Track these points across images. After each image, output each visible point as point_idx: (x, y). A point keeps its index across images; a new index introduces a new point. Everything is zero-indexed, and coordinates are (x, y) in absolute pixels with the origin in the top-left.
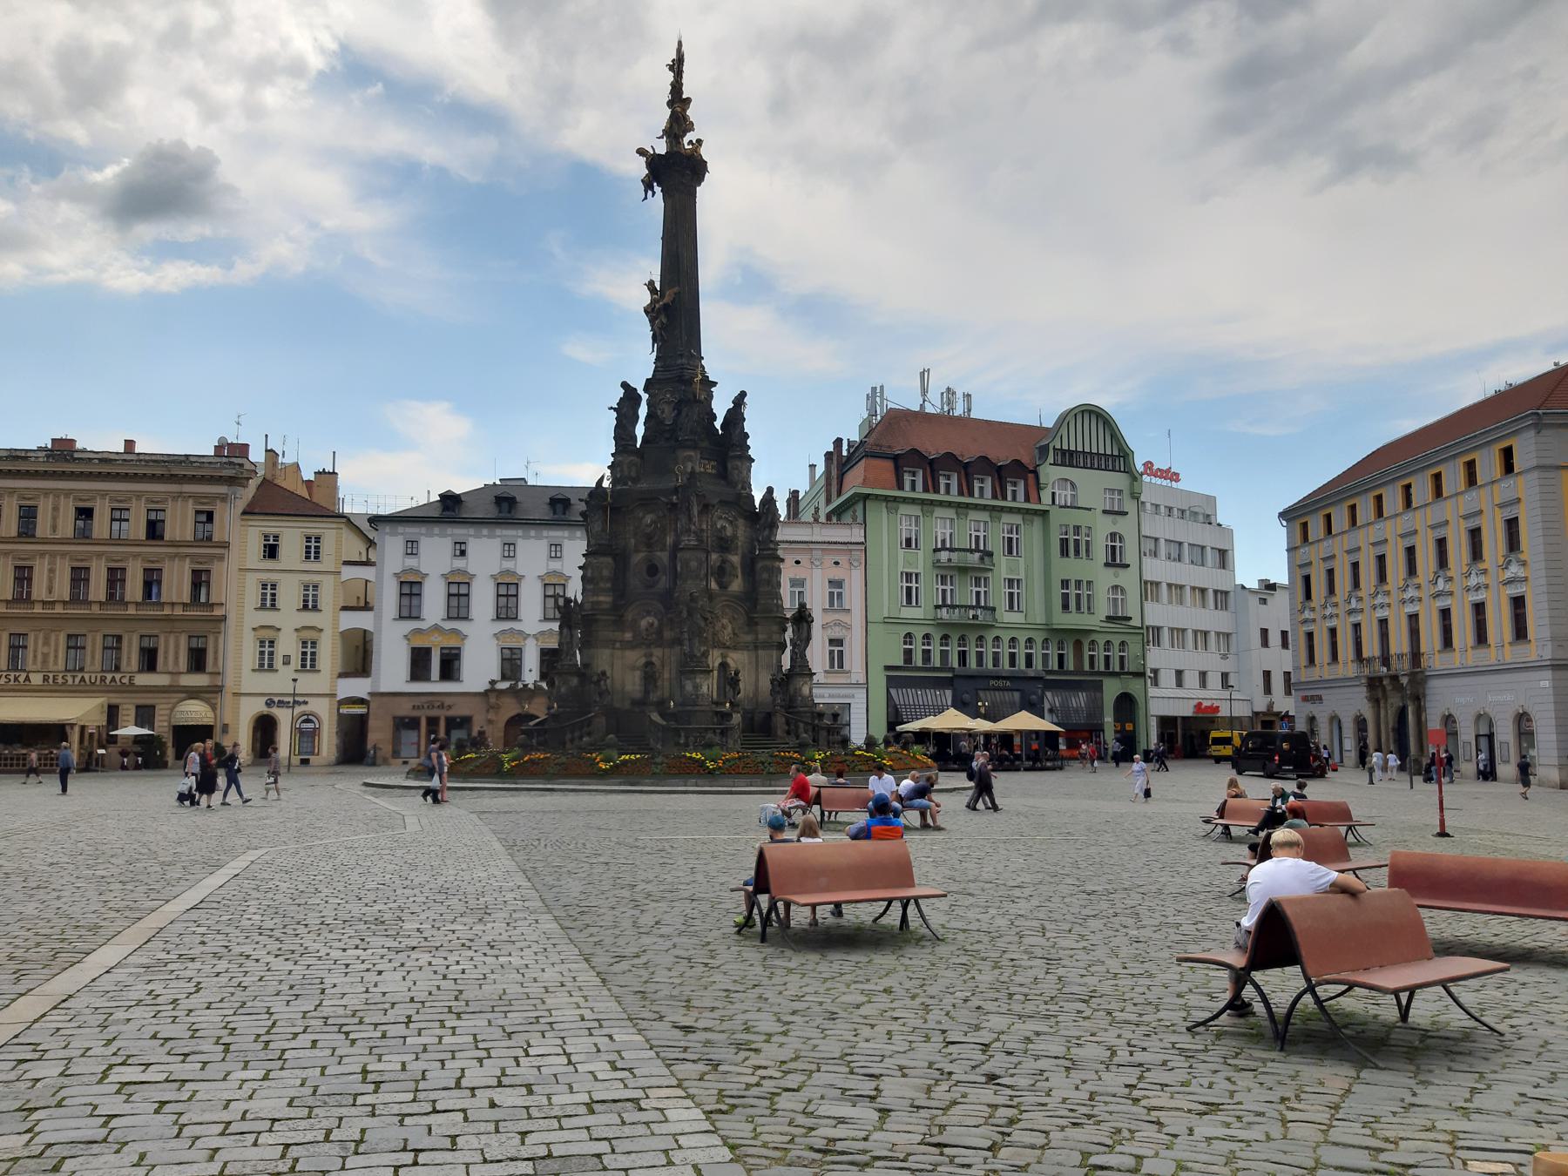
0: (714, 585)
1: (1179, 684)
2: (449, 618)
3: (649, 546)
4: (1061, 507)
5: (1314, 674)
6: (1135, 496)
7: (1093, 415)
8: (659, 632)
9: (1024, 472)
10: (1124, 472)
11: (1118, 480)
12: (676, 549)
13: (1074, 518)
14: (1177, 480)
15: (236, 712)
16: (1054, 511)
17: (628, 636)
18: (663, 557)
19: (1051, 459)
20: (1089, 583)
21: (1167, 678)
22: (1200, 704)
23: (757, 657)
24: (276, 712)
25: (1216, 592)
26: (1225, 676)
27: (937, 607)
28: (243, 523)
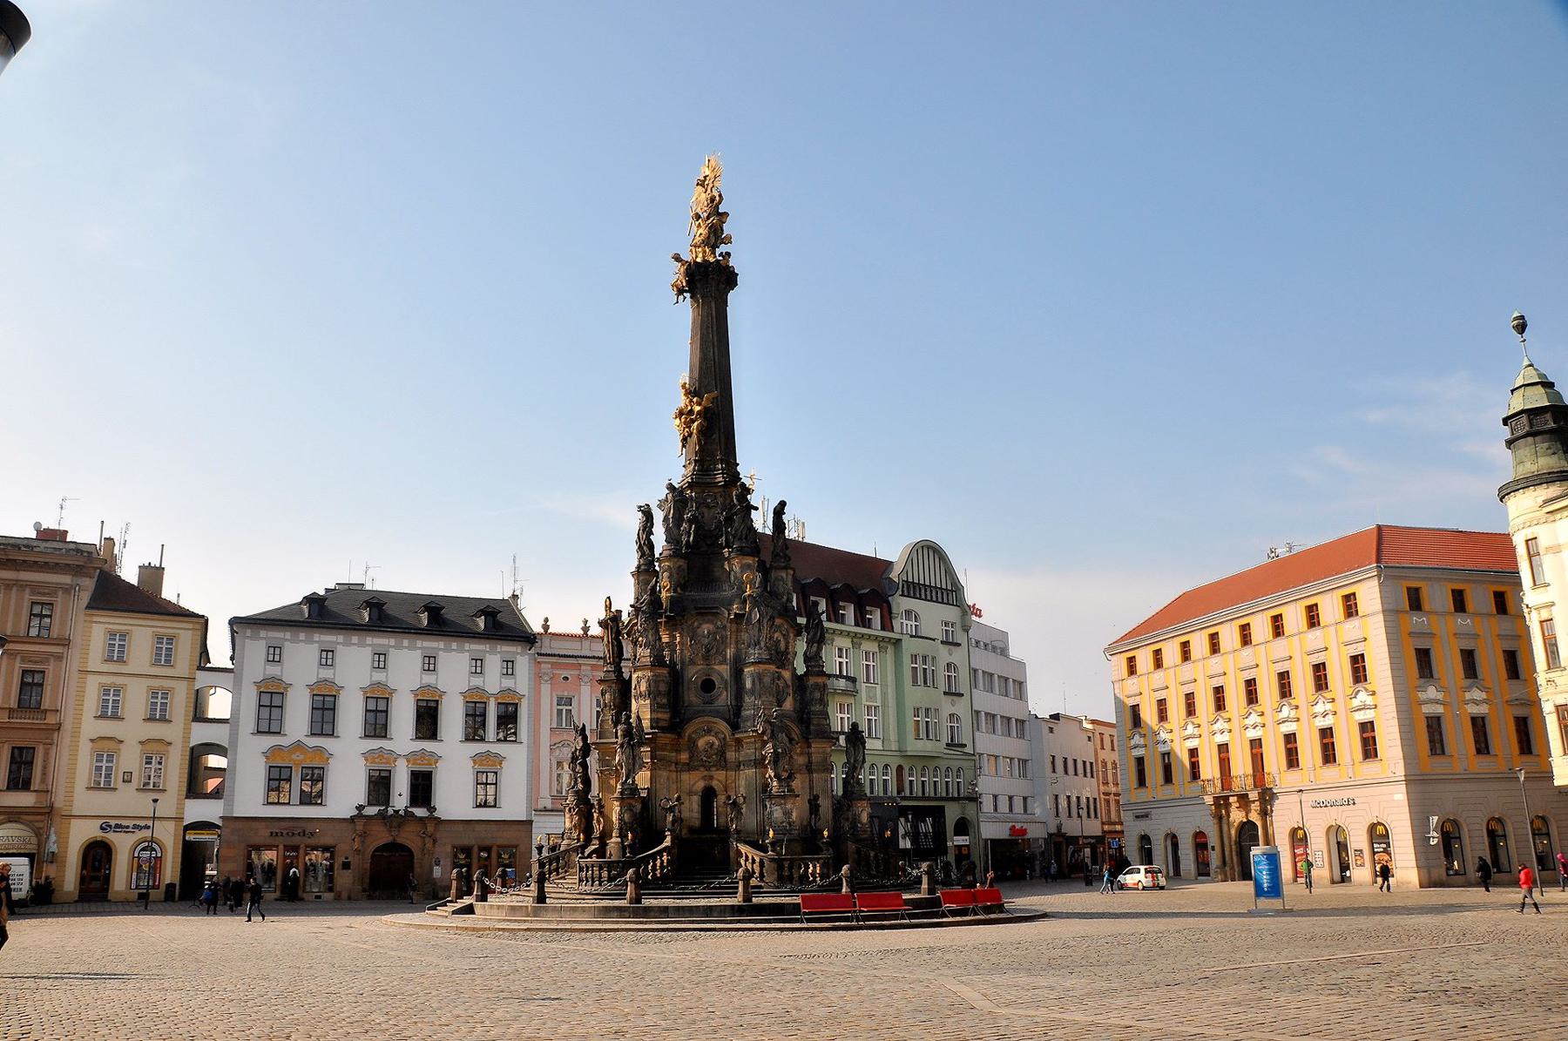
3: (706, 658)
4: (912, 636)
5: (1142, 795)
6: (966, 629)
7: (930, 551)
9: (880, 598)
10: (956, 605)
11: (951, 613)
14: (980, 616)
15: (63, 841)
16: (905, 638)
17: (684, 757)
18: (724, 670)
19: (900, 592)
20: (937, 710)
21: (987, 804)
22: (1014, 826)
23: (811, 781)
24: (112, 837)
25: (1016, 720)
28: (88, 618)
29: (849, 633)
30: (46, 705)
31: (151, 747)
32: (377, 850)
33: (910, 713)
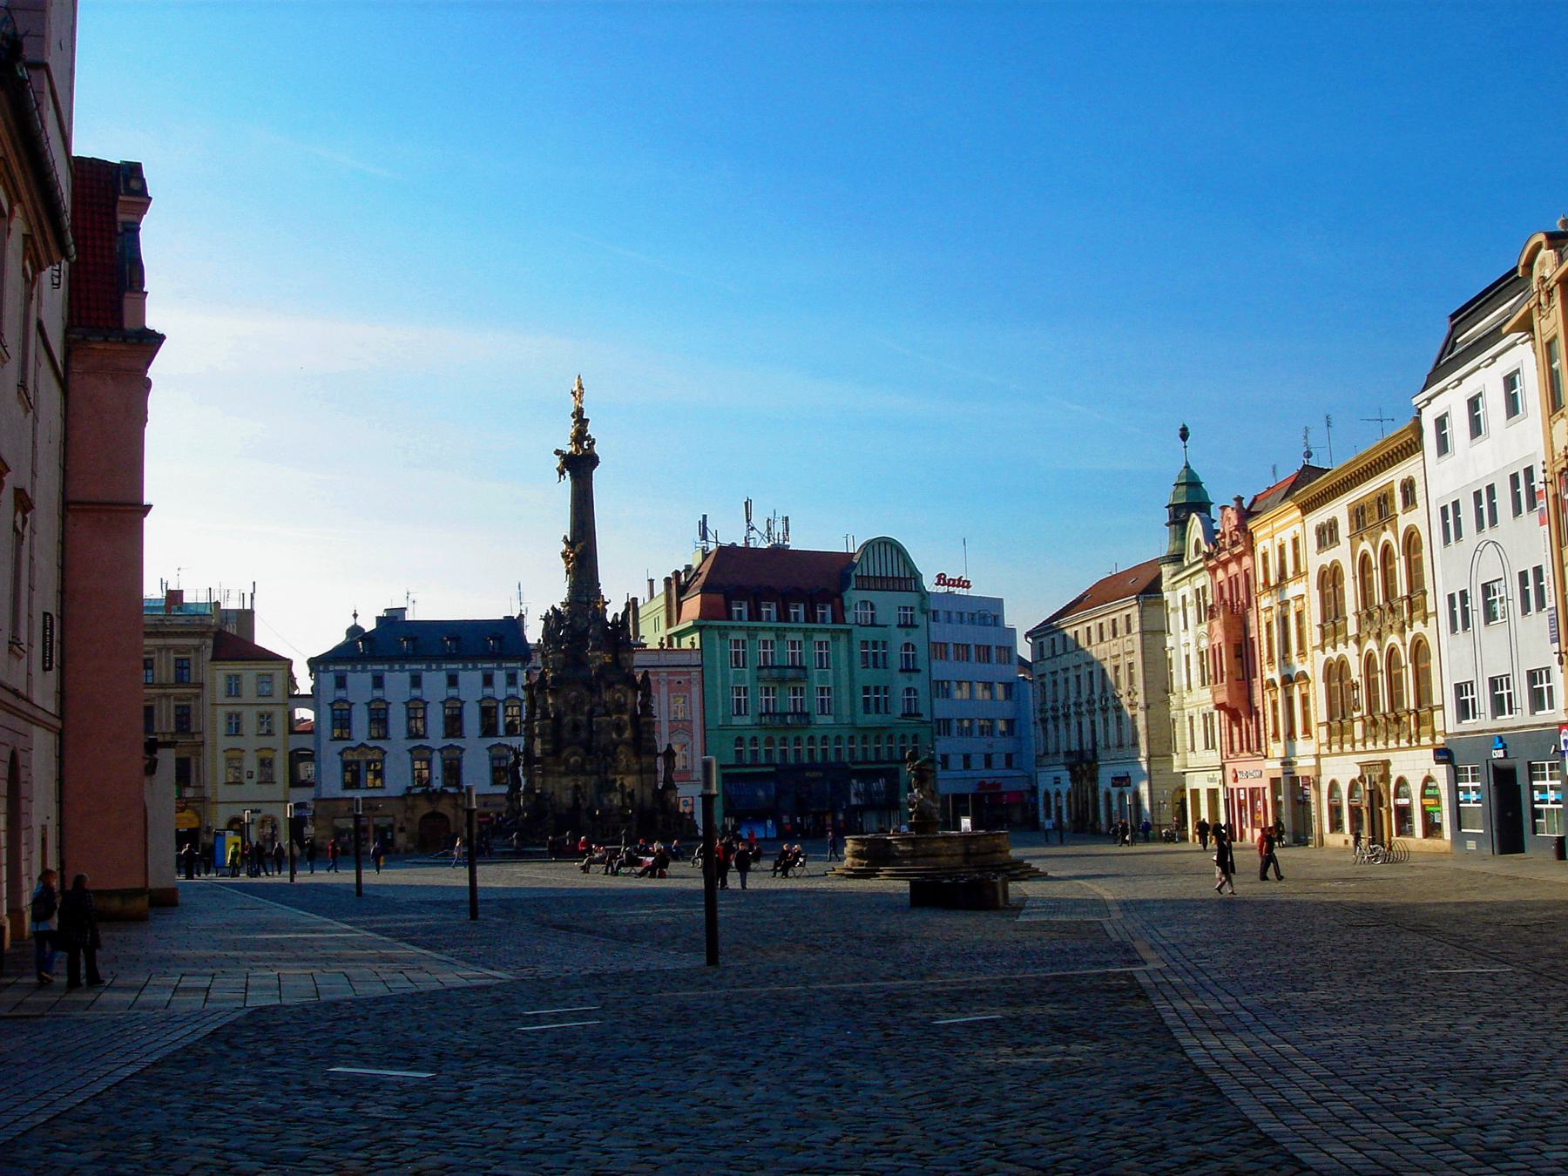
0: (614, 736)
1: (967, 766)
2: (373, 738)
8: (583, 765)
11: (910, 599)
12: (591, 713)
13: (871, 634)
14: (968, 587)
17: (562, 768)
18: (583, 718)
21: (956, 762)
26: (1009, 758)
27: (762, 715)
29: (799, 629)
30: (193, 730)
31: (265, 754)
32: (424, 817)
33: (858, 690)
